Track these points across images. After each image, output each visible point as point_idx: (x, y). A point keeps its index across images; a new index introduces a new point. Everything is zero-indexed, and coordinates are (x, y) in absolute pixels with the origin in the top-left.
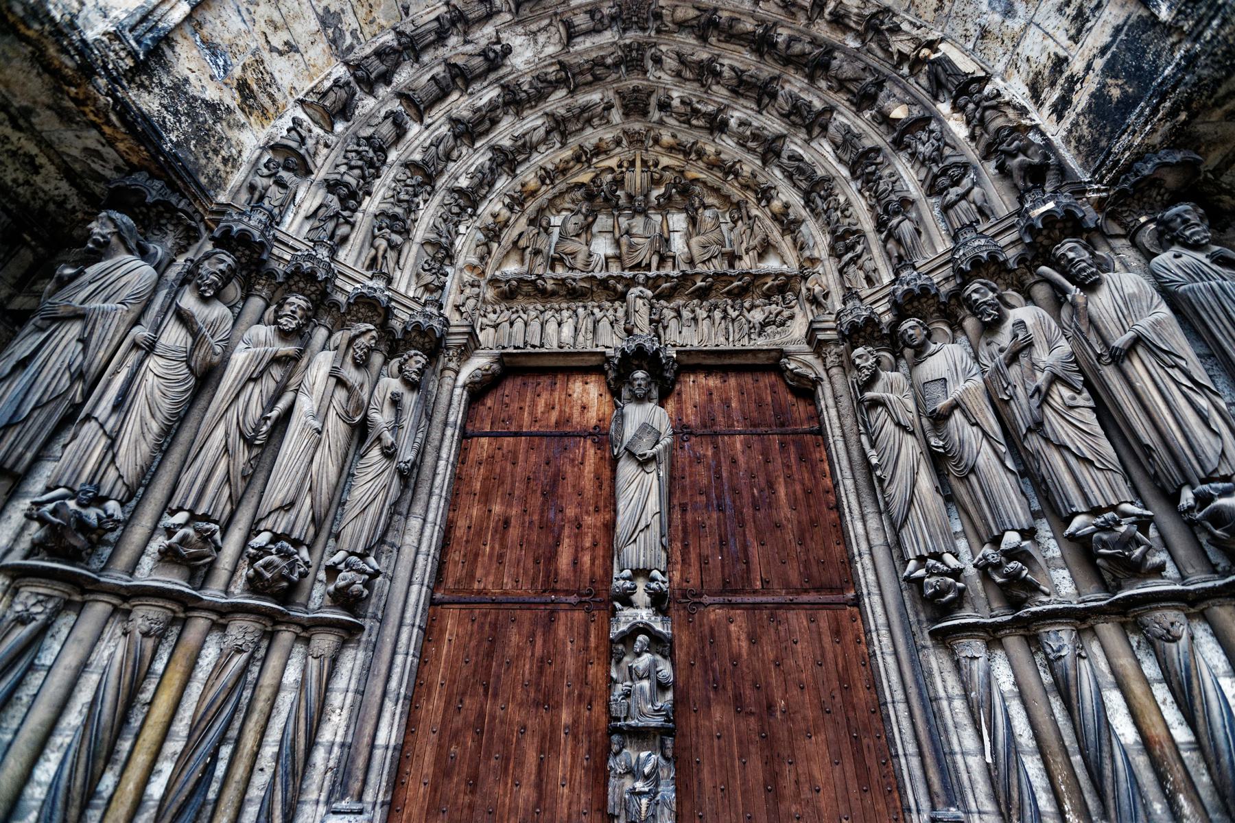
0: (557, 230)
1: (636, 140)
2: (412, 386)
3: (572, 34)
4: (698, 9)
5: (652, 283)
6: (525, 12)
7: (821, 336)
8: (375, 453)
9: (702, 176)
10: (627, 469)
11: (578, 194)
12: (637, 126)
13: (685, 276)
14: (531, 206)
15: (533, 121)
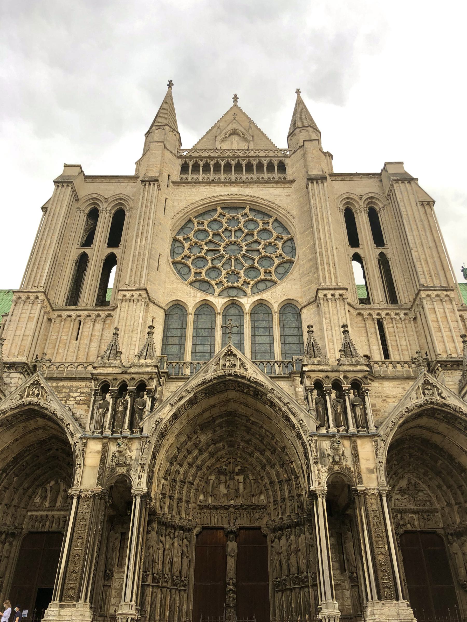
0: (211, 482)
1: (231, 453)
2: (188, 541)
3: (215, 431)
4: (246, 427)
5: (234, 507)
6: (204, 429)
7: (268, 526)
8: (185, 557)
9: (248, 466)
10: (229, 558)
11: (217, 470)
12: (231, 449)
13: (242, 505)
14: (205, 478)
15: (206, 455)
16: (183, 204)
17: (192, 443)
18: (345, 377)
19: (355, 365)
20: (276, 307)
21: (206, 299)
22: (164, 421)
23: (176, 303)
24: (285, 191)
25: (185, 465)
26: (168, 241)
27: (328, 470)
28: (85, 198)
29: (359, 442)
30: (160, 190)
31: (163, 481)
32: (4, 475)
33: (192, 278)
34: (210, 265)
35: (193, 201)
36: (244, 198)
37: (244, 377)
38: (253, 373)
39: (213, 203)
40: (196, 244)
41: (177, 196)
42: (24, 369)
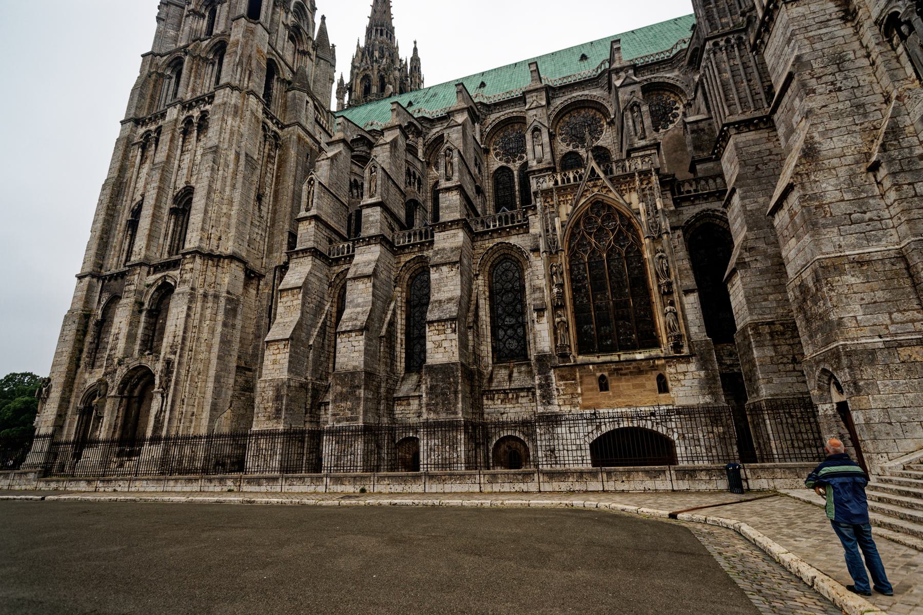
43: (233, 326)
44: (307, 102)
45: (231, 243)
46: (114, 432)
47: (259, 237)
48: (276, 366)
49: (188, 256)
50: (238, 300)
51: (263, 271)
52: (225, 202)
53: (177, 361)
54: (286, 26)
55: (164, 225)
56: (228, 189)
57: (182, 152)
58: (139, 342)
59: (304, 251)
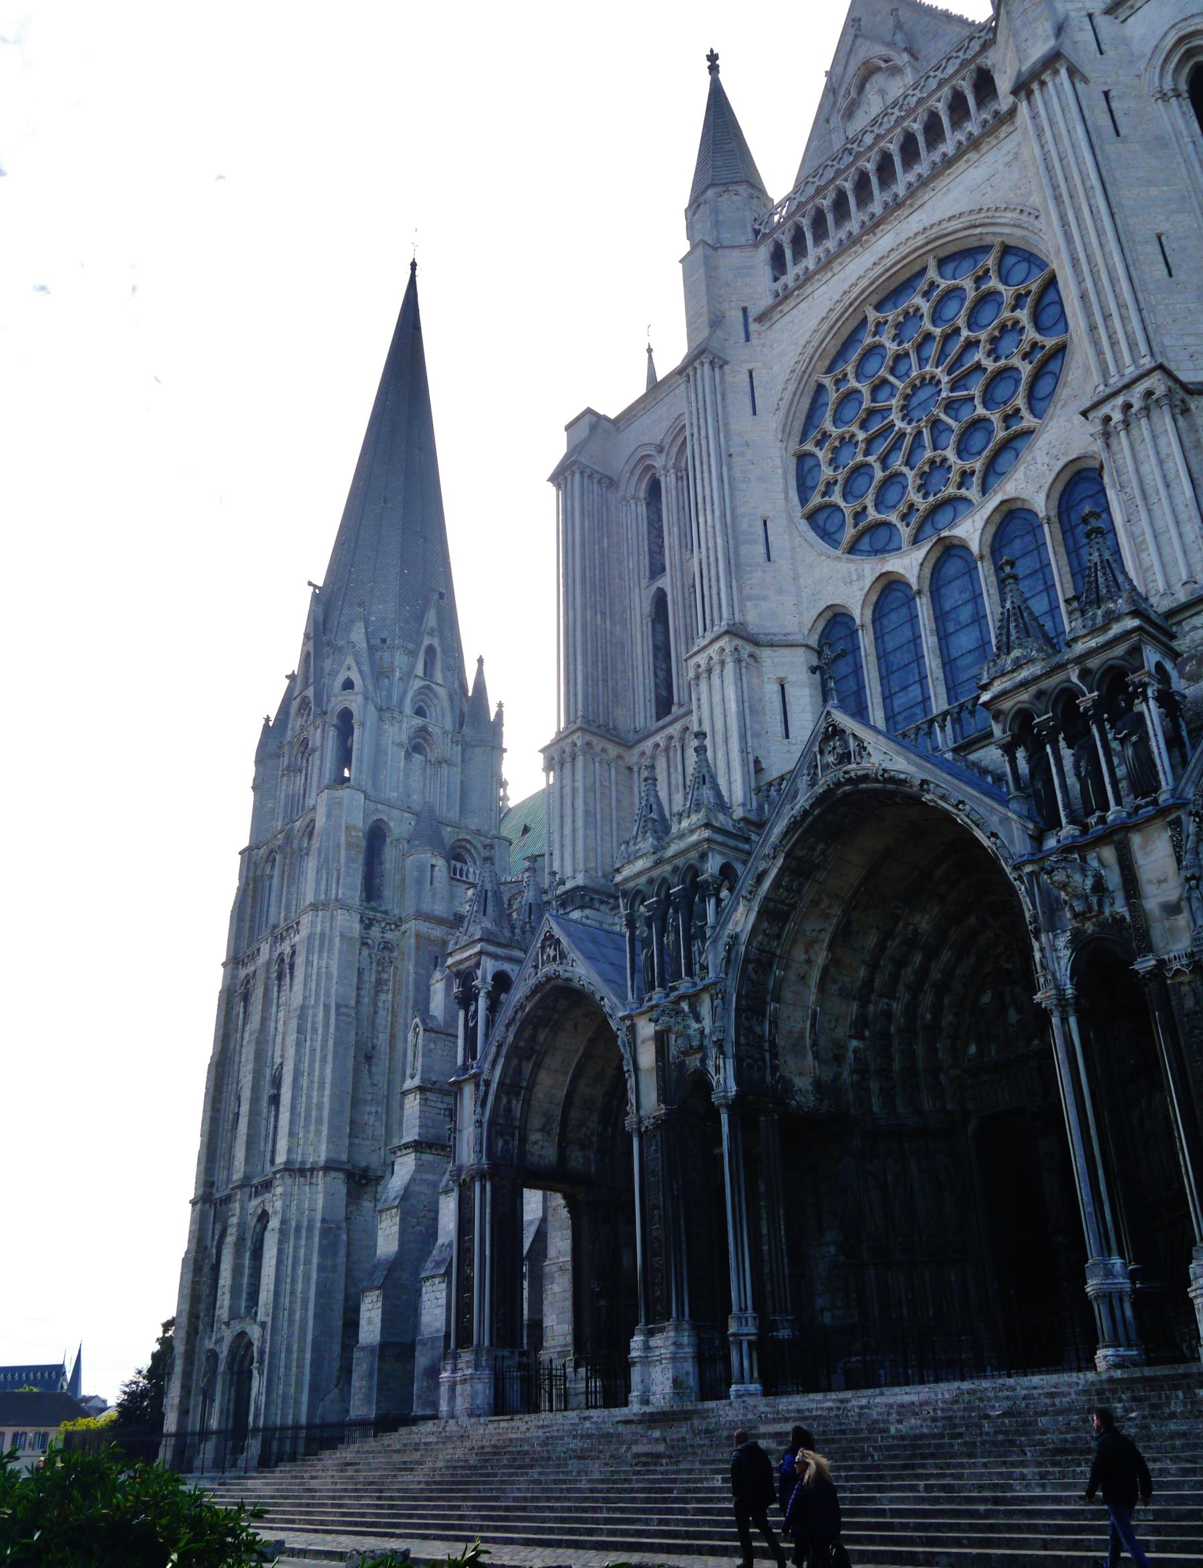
15: (946, 955)
16: (789, 361)
17: (897, 941)
18: (1084, 674)
19: (1105, 628)
20: (1040, 504)
21: (884, 571)
22: (744, 938)
23: (829, 615)
24: (1003, 151)
25: (903, 994)
26: (780, 471)
27: (1071, 942)
28: (627, 467)
29: (1136, 840)
30: (727, 363)
31: (854, 1043)
32: (615, 1102)
33: (850, 532)
34: (879, 474)
35: (806, 338)
36: (912, 245)
37: (865, 778)
38: (883, 756)
39: (851, 310)
40: (842, 439)
41: (775, 345)
42: (587, 899)
43: (335, 1266)
44: (433, 866)
45: (323, 1147)
46: (227, 1420)
47: (372, 1119)
48: (371, 1328)
49: (278, 1176)
50: (339, 1228)
51: (379, 1173)
52: (316, 1086)
53: (269, 1325)
54: (400, 745)
55: (264, 1122)
56: (317, 1065)
57: (278, 1006)
58: (244, 1296)
59: (406, 1146)
